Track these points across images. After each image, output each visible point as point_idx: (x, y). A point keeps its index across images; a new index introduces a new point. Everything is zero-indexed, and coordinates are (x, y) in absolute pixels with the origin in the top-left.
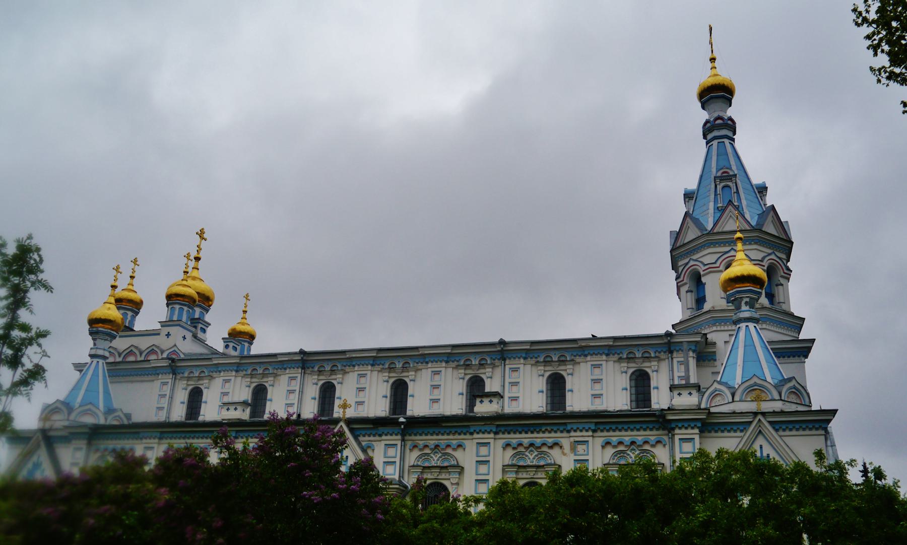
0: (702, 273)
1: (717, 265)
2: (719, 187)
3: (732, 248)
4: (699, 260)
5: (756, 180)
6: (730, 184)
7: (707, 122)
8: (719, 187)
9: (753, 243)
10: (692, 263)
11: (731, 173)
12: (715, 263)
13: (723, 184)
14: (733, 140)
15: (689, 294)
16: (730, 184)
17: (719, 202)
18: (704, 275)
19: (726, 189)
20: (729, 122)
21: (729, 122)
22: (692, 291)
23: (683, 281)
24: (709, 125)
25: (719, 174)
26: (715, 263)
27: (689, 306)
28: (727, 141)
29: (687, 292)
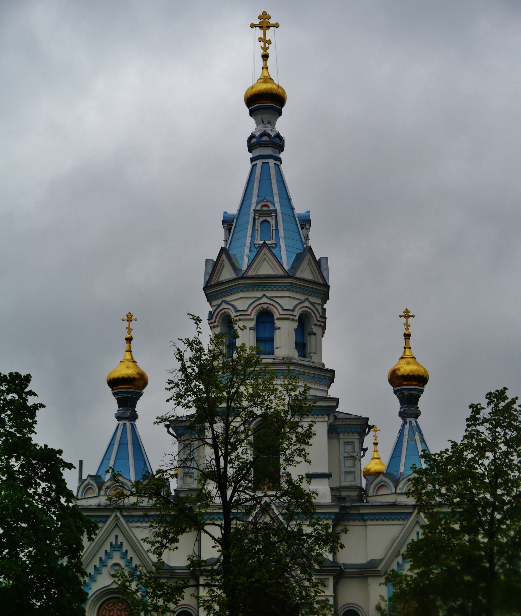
2: (258, 223)
3: (264, 295)
4: (232, 303)
5: (299, 209)
6: (269, 219)
7: (252, 136)
8: (258, 223)
9: (285, 289)
11: (272, 208)
13: (262, 219)
16: (269, 219)
17: (256, 239)
19: (266, 224)
20: (277, 140)
21: (277, 140)
23: (215, 322)
24: (254, 140)
25: (259, 208)
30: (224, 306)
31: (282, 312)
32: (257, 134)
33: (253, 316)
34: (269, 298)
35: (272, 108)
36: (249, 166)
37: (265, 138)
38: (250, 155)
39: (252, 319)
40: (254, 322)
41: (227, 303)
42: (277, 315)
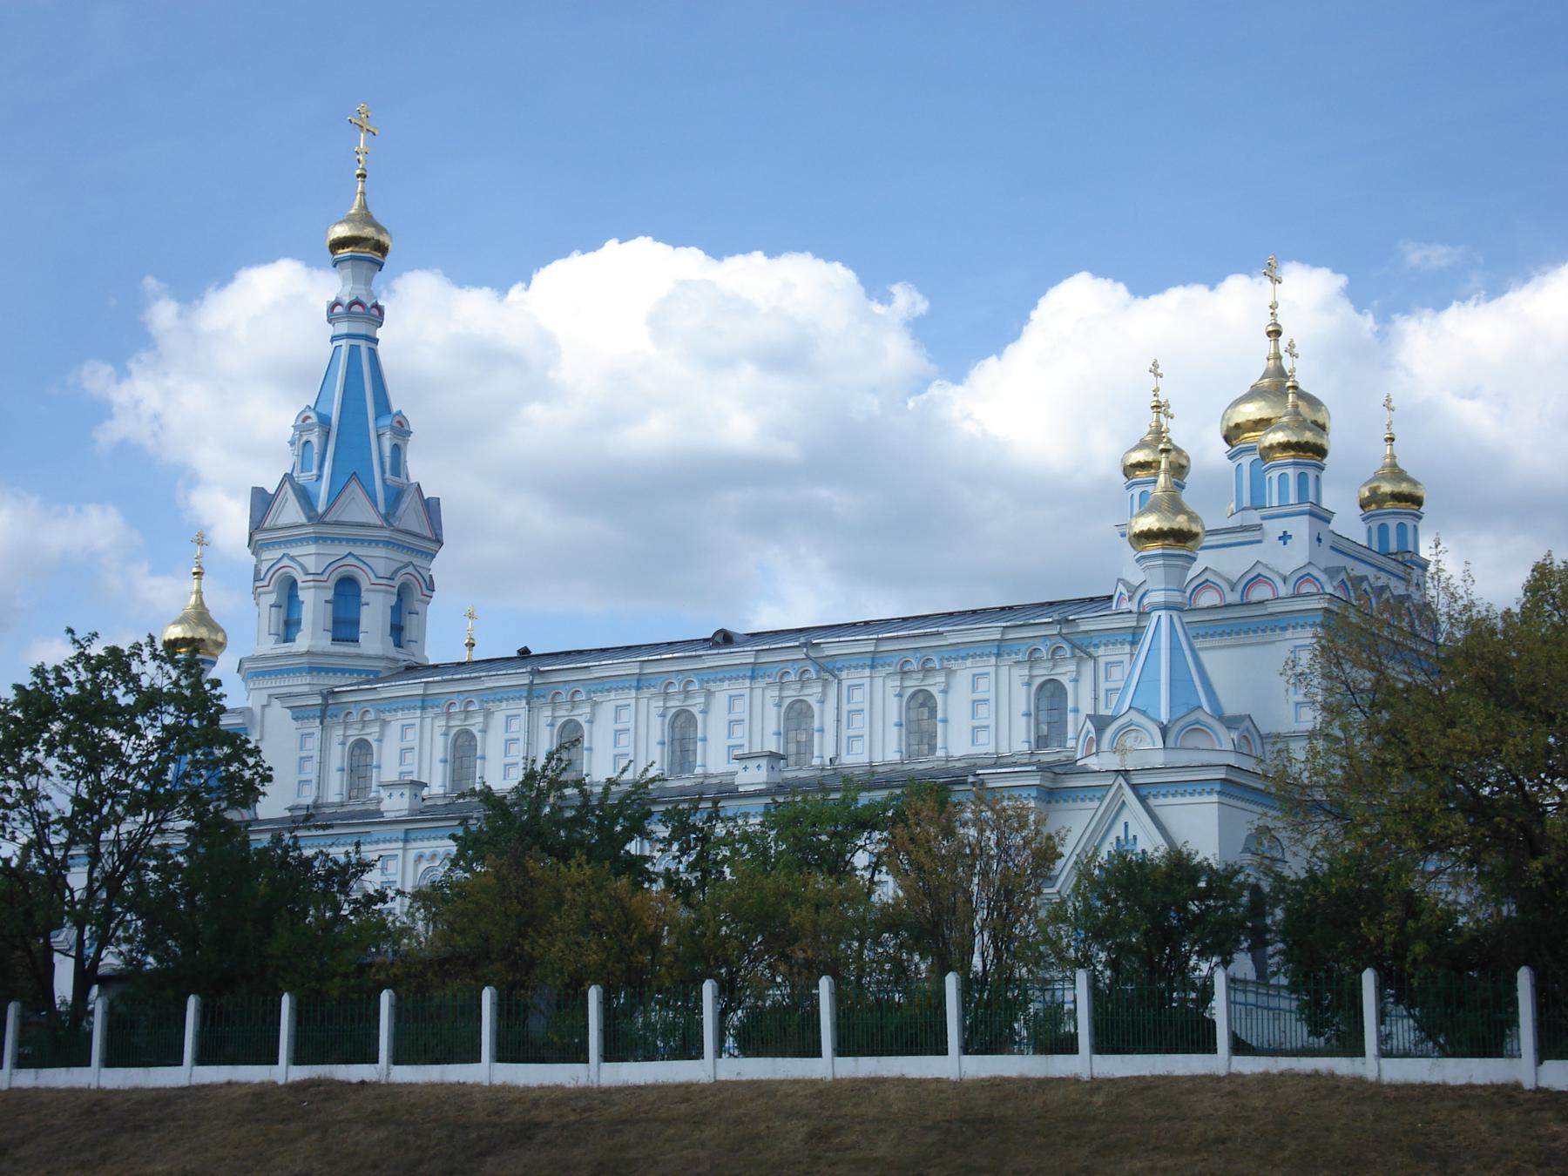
0: (300, 584)
1: (324, 578)
3: (350, 553)
4: (300, 559)
7: (336, 304)
10: (286, 562)
12: (322, 574)
14: (376, 341)
15: (273, 609)
18: (303, 589)
22: (280, 607)
24: (338, 309)
26: (322, 574)
27: (272, 632)
28: (363, 344)
29: (271, 606)
30: (286, 562)
31: (374, 580)
32: (346, 300)
33: (331, 583)
34: (357, 557)
35: (371, 260)
36: (329, 348)
37: (357, 308)
38: (330, 330)
39: (330, 588)
40: (332, 592)
41: (292, 558)
42: (365, 584)
